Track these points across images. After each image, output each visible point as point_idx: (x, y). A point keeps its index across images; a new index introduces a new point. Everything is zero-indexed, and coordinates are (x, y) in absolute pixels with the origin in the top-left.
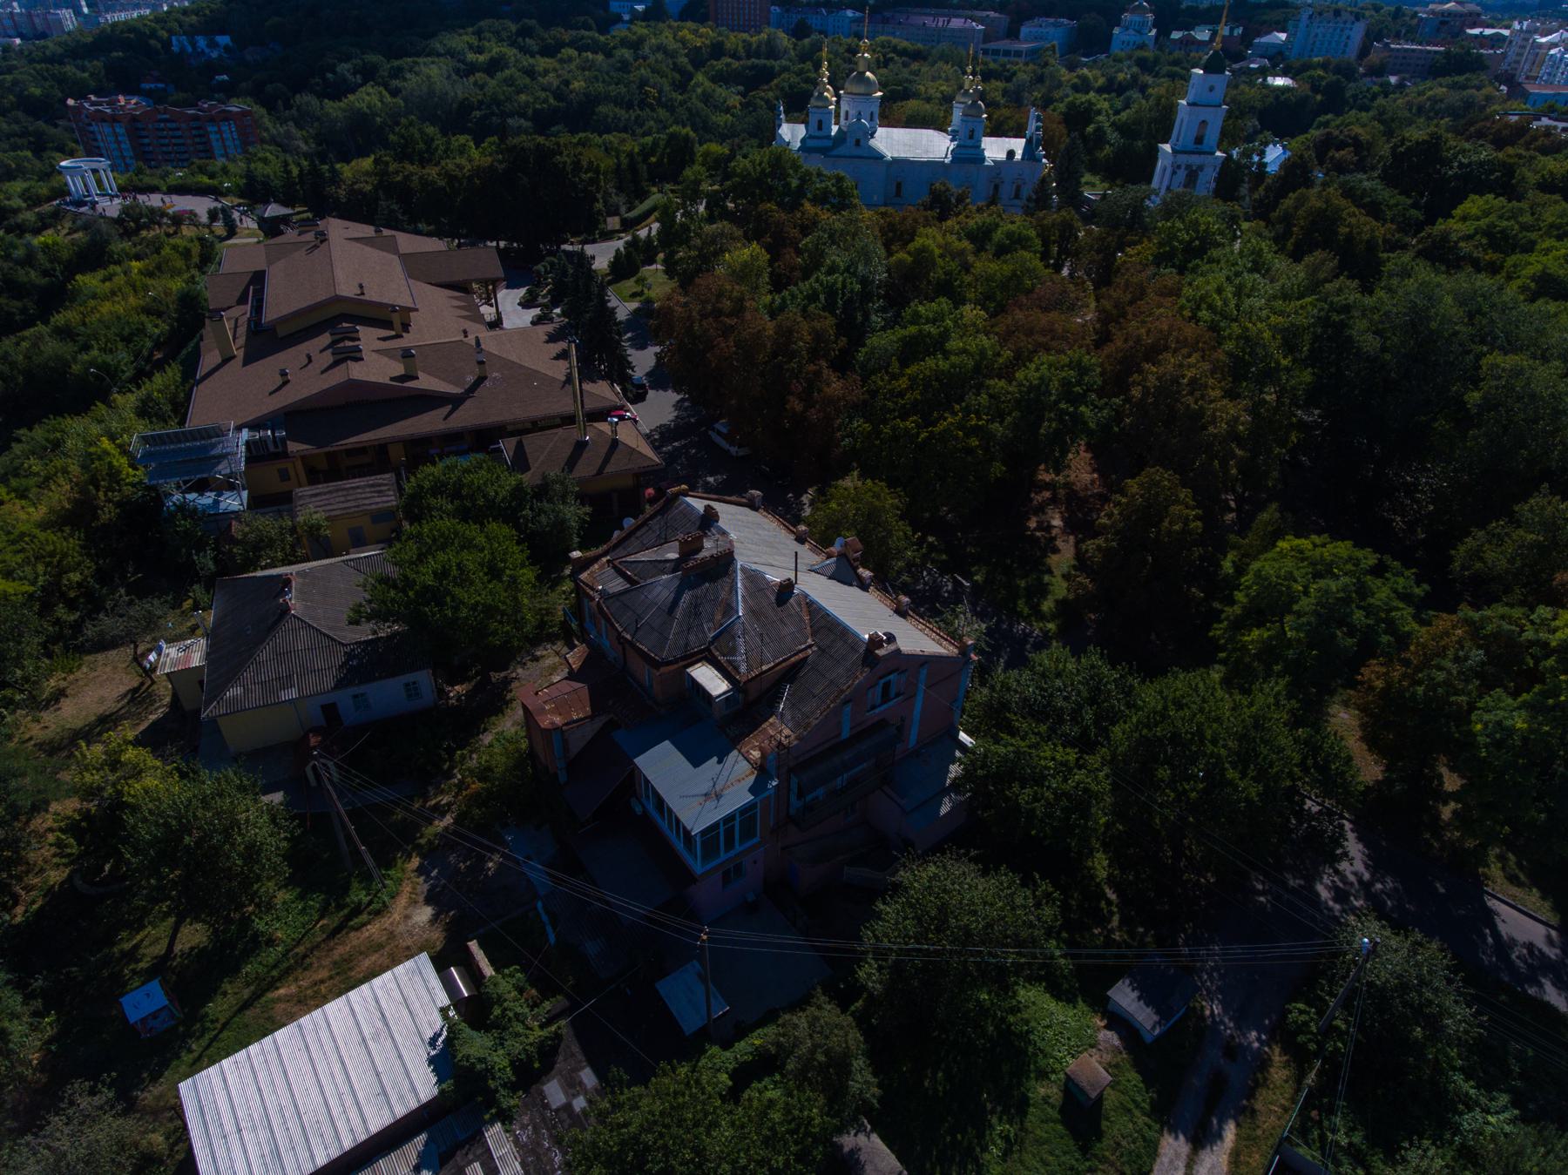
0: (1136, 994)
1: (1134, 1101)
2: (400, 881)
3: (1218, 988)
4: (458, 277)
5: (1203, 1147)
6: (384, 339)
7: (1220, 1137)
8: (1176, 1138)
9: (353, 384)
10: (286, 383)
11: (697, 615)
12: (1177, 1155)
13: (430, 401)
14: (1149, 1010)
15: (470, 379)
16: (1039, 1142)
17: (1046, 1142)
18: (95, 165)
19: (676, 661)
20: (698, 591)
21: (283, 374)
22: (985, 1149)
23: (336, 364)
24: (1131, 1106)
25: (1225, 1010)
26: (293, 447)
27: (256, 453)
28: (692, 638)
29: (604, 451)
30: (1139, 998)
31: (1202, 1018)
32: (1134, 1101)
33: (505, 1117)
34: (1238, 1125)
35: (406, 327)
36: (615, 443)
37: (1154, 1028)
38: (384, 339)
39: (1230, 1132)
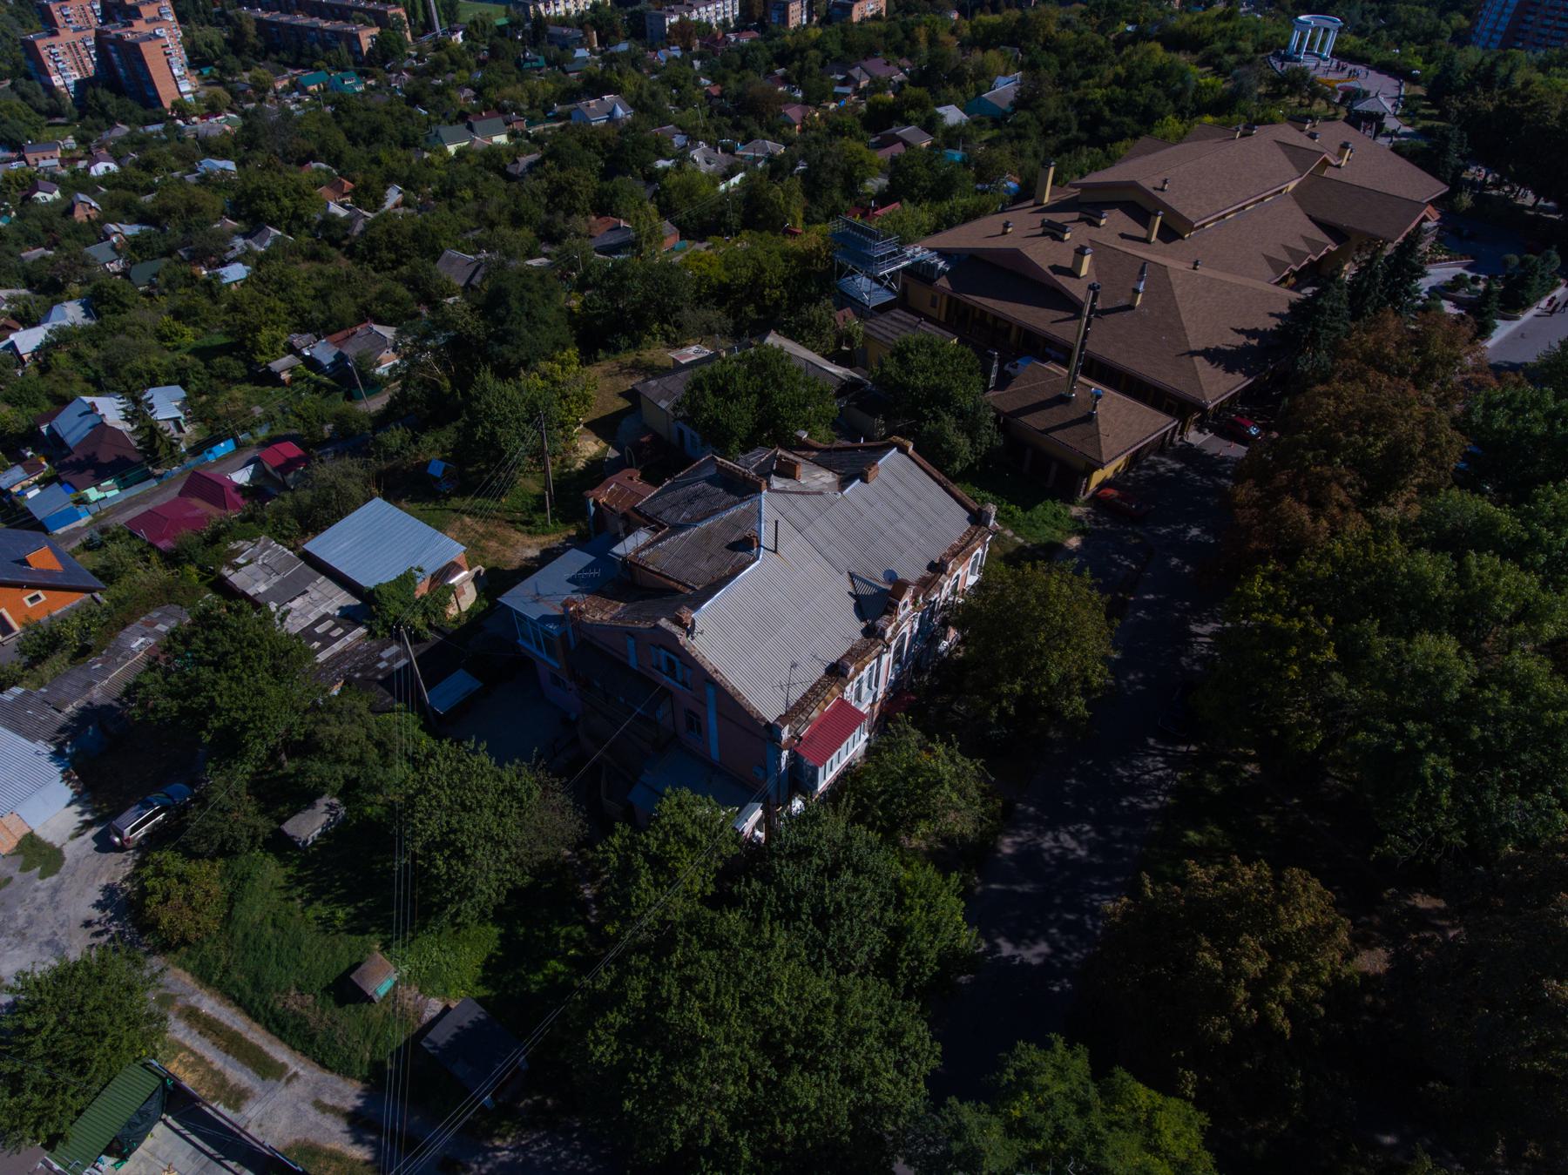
0: (466, 1024)
1: (378, 1038)
2: (556, 531)
3: (530, 1161)
4: (1345, 222)
5: (350, 1124)
6: (1123, 236)
7: (359, 1141)
8: (359, 1097)
9: (1016, 254)
10: (1004, 233)
11: (690, 502)
12: (344, 1098)
13: (1070, 305)
14: (448, 1037)
15: (1123, 302)
16: (334, 948)
17: (333, 953)
18: (1328, 25)
19: (643, 515)
20: (711, 489)
21: (1006, 226)
22: (326, 903)
23: (1044, 234)
24: (372, 1038)
25: (503, 1164)
26: (943, 282)
27: (919, 273)
28: (669, 512)
29: (1073, 416)
30: (461, 1028)
31: (490, 1136)
32: (378, 1038)
33: (372, 634)
34: (367, 1163)
35: (1170, 233)
36: (1089, 418)
37: (429, 1041)
38: (1123, 236)
39: (361, 1153)
